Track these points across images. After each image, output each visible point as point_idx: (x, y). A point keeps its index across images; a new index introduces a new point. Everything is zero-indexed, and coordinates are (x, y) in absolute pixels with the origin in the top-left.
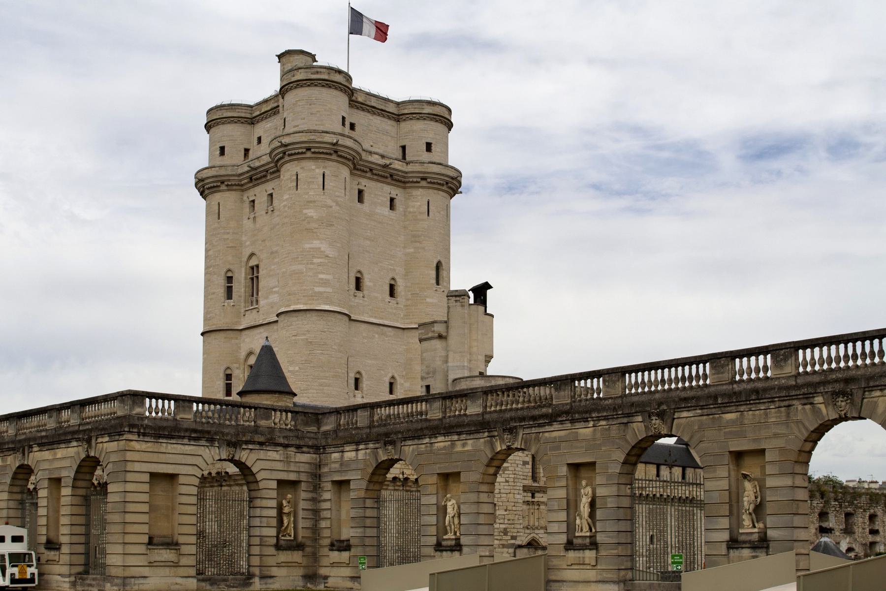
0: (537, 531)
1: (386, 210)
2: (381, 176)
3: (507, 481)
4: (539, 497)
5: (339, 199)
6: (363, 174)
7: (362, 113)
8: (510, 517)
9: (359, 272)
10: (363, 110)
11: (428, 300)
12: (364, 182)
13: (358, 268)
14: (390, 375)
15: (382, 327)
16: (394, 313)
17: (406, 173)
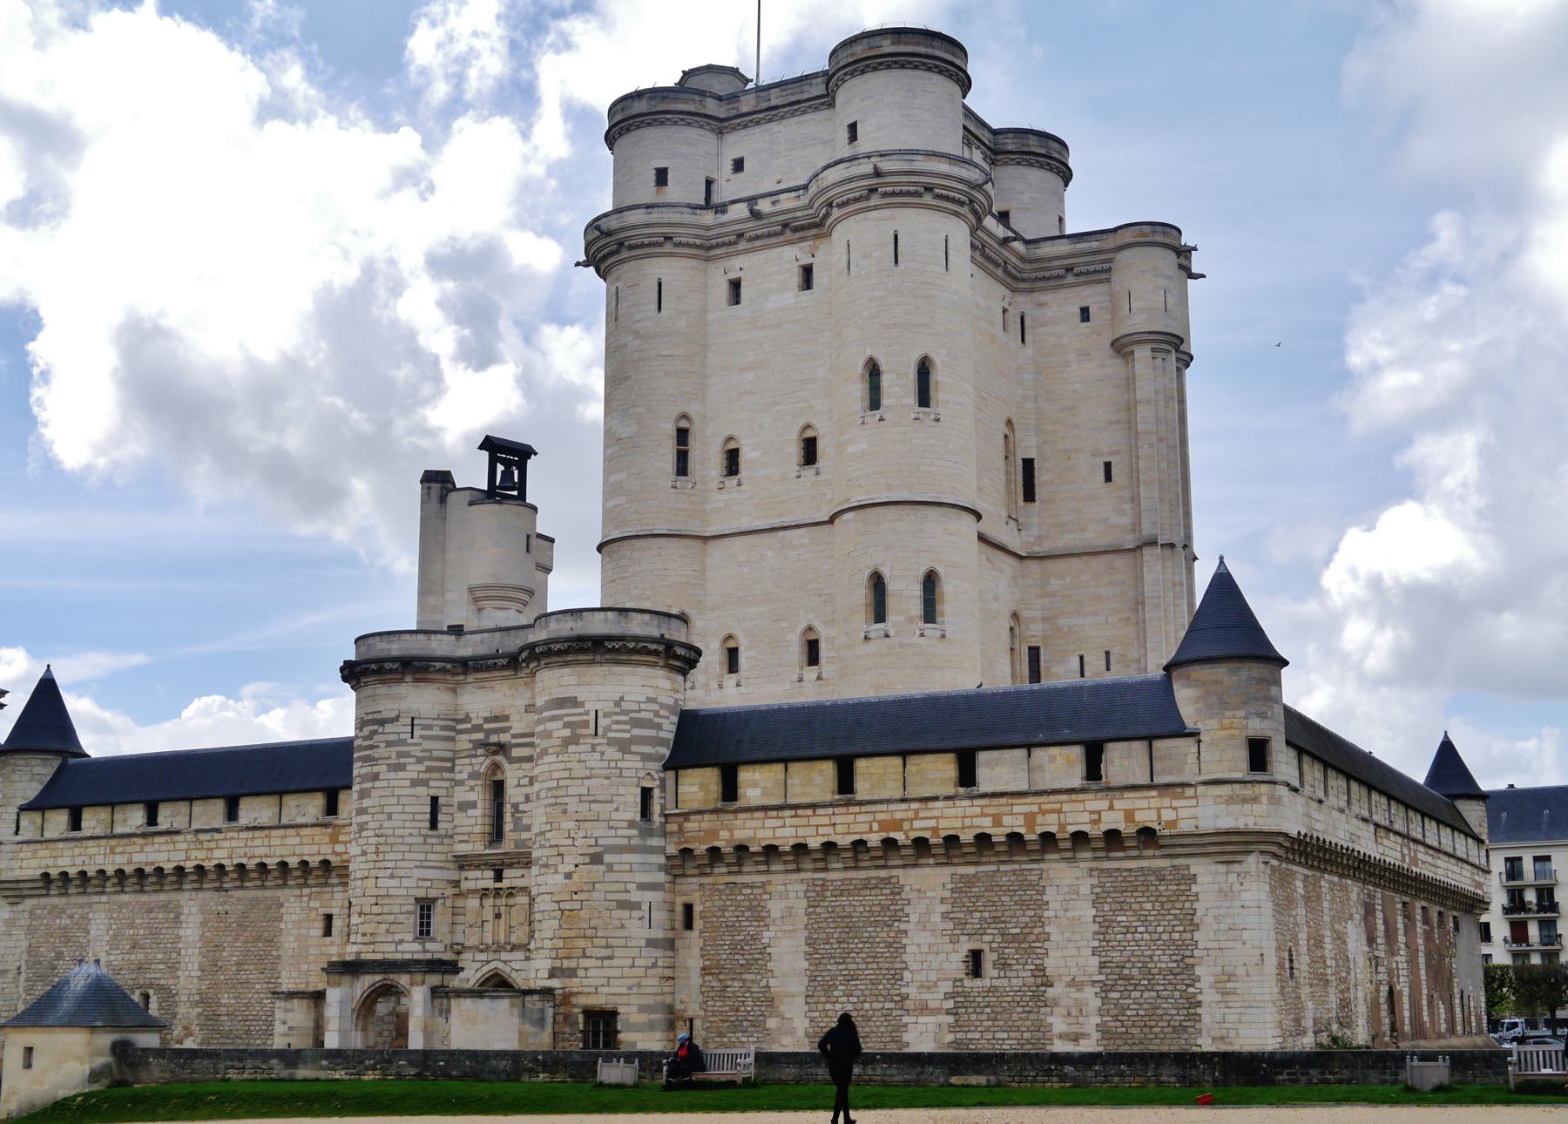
0: (504, 956)
1: (790, 296)
2: (769, 235)
3: (364, 853)
4: (511, 877)
5: (639, 325)
6: (732, 249)
7: (758, 129)
8: (368, 929)
9: (730, 439)
10: (758, 123)
11: (851, 449)
12: (737, 262)
13: (728, 433)
14: (803, 626)
15: (781, 534)
16: (811, 495)
17: (810, 206)
